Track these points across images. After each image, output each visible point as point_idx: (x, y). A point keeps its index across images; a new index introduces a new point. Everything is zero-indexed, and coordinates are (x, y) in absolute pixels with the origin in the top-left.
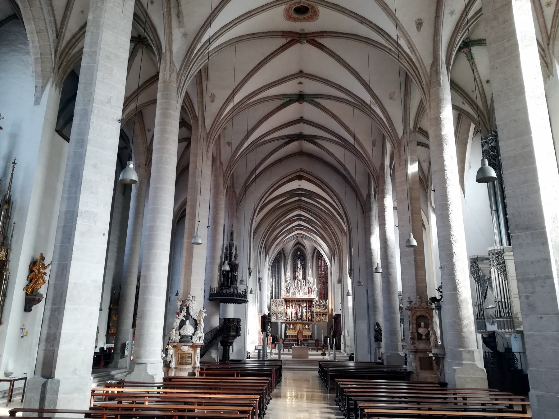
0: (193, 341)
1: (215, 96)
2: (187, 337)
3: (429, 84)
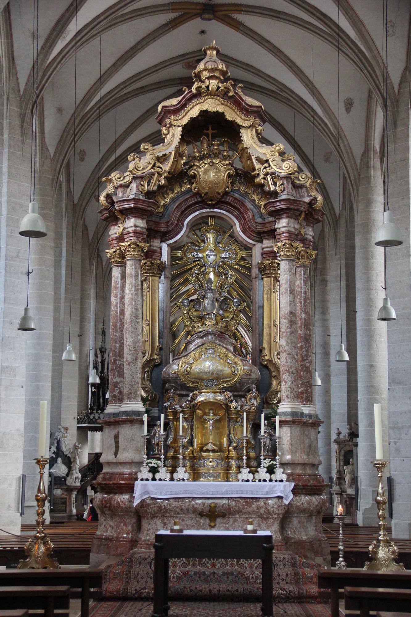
0: (68, 483)
1: (85, 153)
2: (60, 478)
3: (357, 180)
